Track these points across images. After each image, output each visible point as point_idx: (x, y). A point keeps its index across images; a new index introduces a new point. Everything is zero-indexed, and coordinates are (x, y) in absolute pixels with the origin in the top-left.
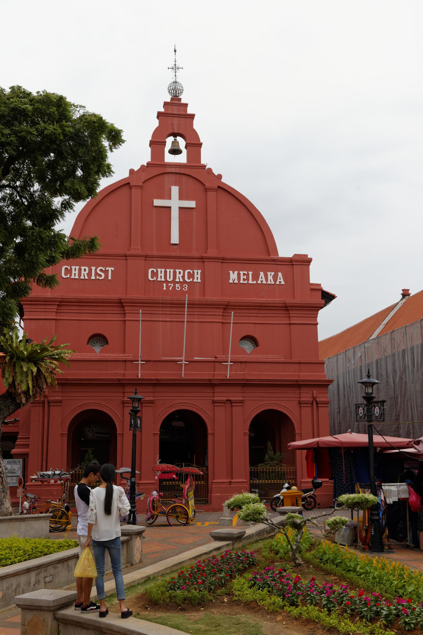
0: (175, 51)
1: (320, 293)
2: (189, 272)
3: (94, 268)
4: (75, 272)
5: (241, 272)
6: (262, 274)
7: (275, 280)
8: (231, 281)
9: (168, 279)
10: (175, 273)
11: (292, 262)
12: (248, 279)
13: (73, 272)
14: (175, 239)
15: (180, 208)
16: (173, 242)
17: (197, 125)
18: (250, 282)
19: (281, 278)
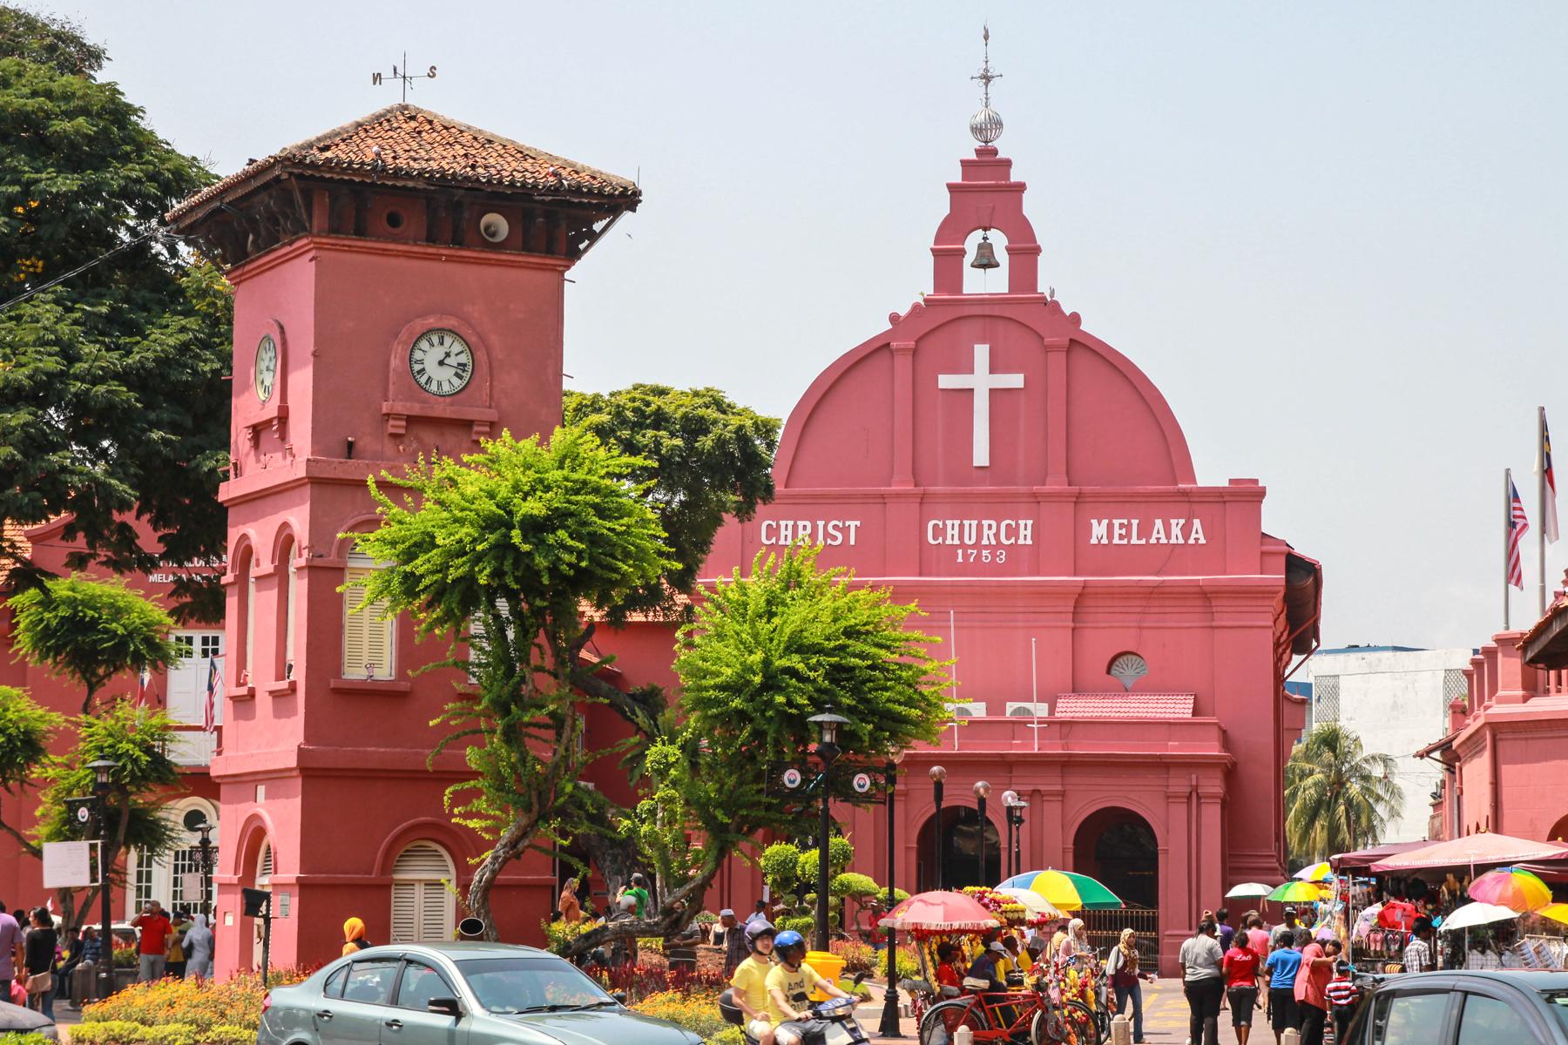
0: (986, 37)
1: (1282, 561)
2: (1008, 526)
3: (823, 522)
4: (786, 533)
5: (1114, 521)
6: (1159, 523)
7: (1186, 535)
8: (1094, 541)
9: (967, 541)
10: (980, 527)
11: (1223, 497)
12: (1129, 535)
13: (783, 533)
14: (981, 456)
15: (990, 390)
16: (975, 465)
17: (1031, 207)
18: (1134, 541)
19: (1200, 531)
